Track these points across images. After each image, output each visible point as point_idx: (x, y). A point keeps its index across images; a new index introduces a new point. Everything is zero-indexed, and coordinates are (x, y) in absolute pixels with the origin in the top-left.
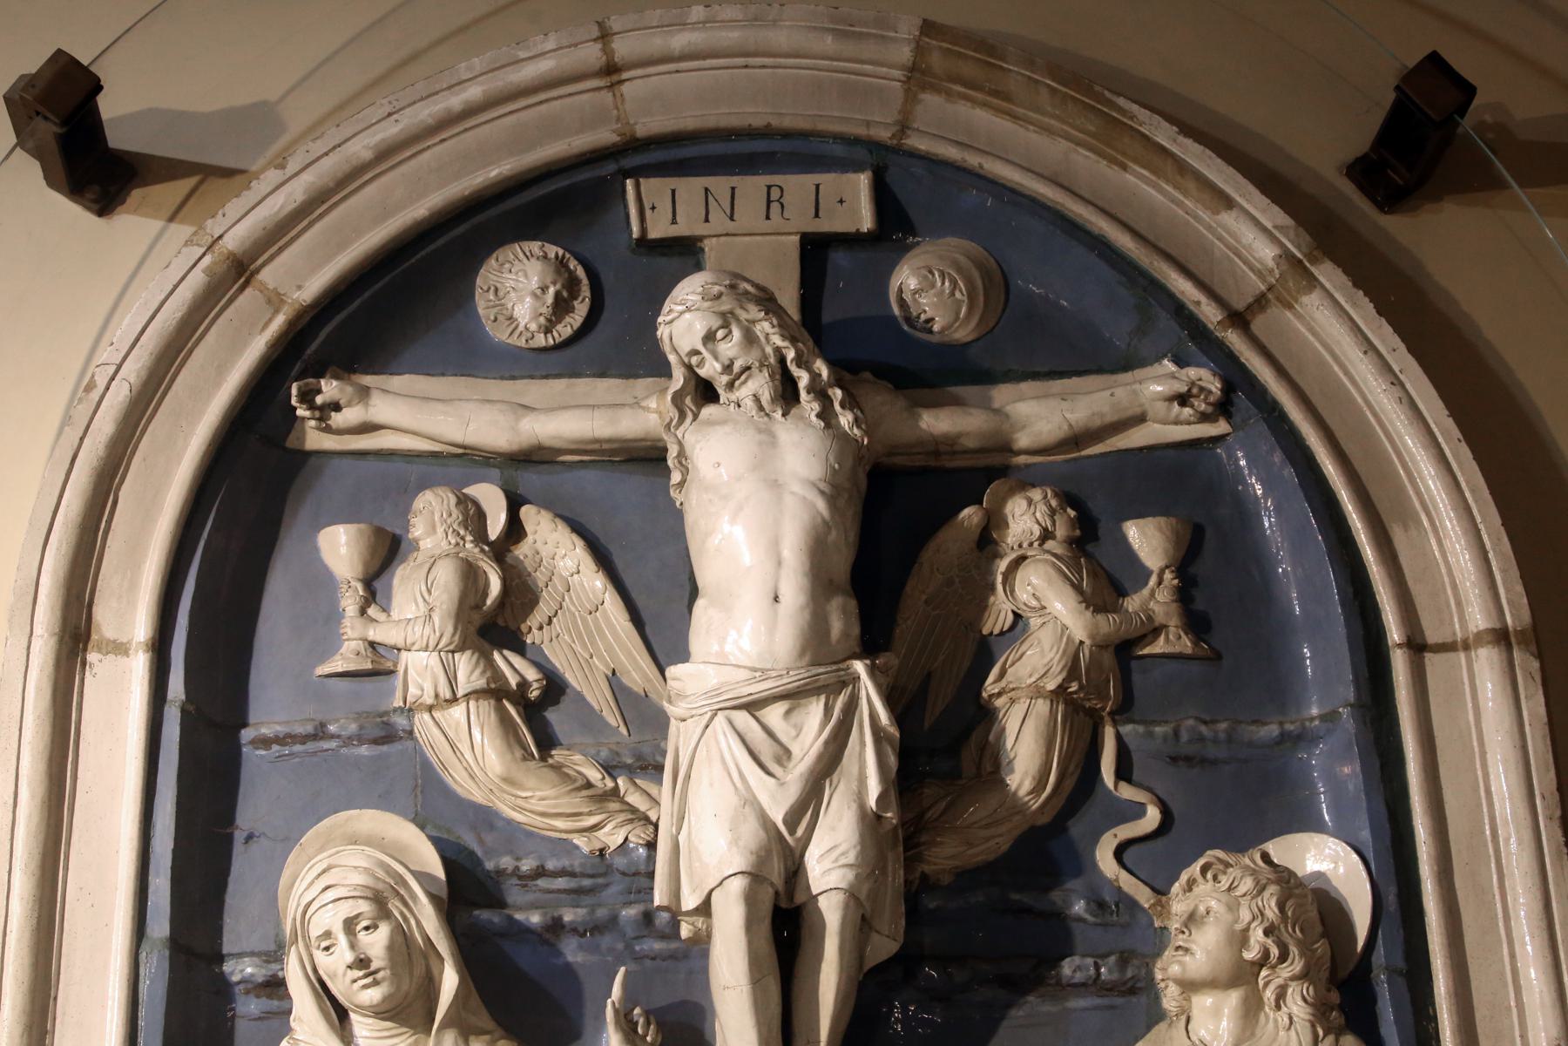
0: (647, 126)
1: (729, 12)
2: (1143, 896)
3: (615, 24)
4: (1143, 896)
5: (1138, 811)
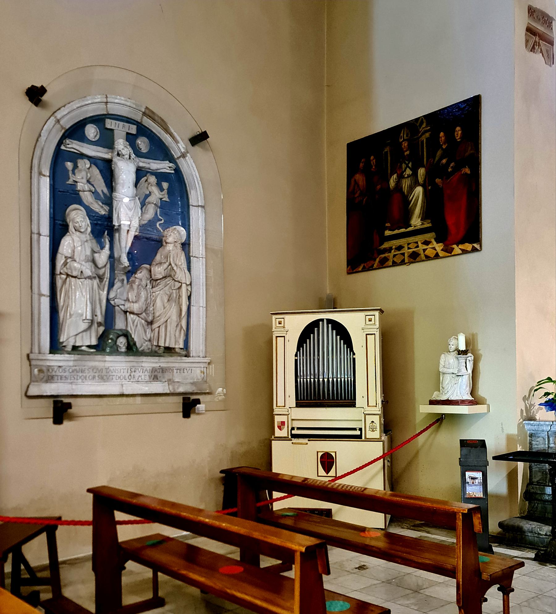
0: (111, 112)
1: (123, 98)
2: (162, 231)
3: (108, 96)
4: (162, 231)
5: (161, 220)
